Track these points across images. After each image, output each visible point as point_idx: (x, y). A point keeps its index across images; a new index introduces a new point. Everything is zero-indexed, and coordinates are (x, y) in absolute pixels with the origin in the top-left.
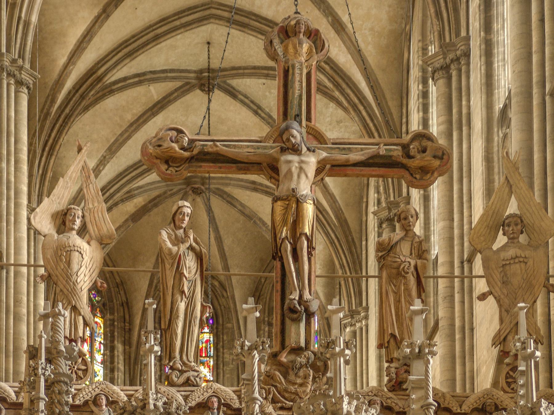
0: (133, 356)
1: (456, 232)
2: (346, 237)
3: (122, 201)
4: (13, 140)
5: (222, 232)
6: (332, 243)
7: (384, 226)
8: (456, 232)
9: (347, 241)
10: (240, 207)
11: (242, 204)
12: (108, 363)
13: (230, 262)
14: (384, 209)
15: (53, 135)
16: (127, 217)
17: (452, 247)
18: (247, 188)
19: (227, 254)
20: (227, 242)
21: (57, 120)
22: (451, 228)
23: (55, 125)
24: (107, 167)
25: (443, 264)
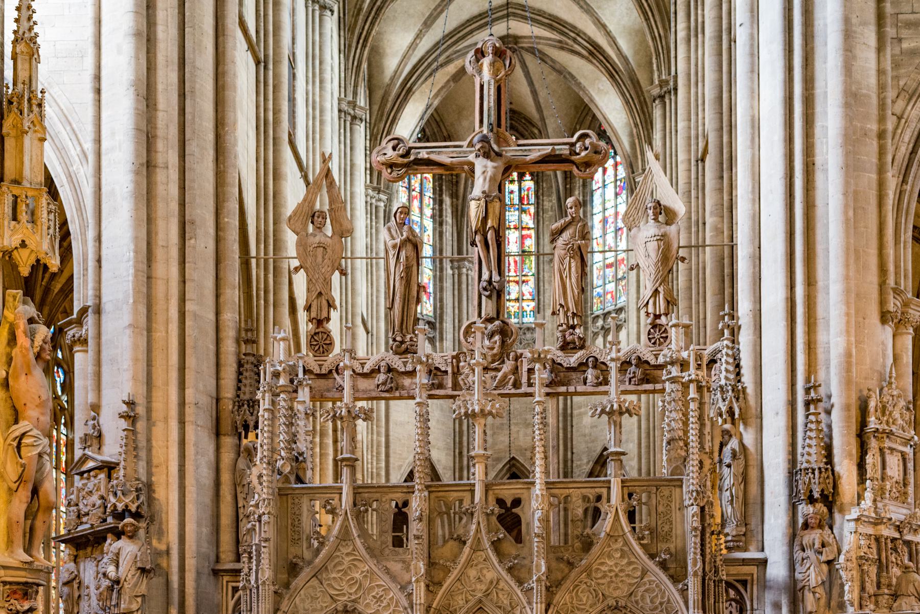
0: (460, 208)
1: (693, 132)
2: (638, 97)
3: (441, 66)
4: (317, 62)
5: (537, 86)
6: (627, 102)
7: (657, 102)
8: (693, 132)
9: (640, 102)
10: (551, 63)
11: (553, 61)
12: (437, 218)
13: (545, 113)
14: (656, 86)
15: (366, 27)
16: (448, 77)
17: (690, 145)
18: (555, 47)
19: (543, 106)
20: (542, 94)
21: (370, 13)
22: (690, 128)
23: (368, 17)
24: (424, 39)
25: (682, 162)
